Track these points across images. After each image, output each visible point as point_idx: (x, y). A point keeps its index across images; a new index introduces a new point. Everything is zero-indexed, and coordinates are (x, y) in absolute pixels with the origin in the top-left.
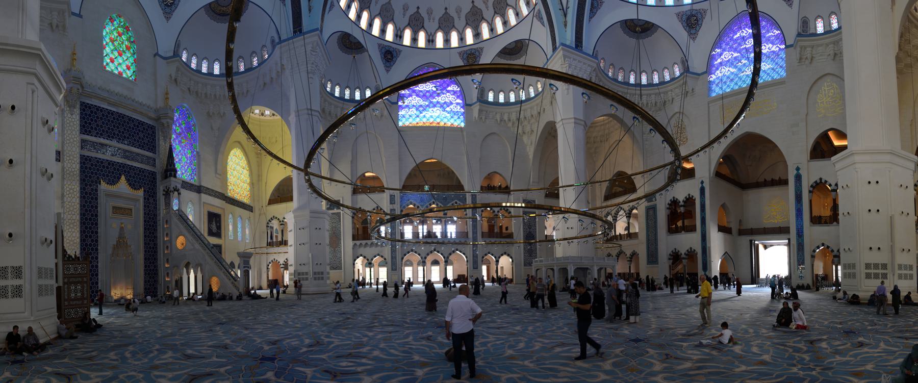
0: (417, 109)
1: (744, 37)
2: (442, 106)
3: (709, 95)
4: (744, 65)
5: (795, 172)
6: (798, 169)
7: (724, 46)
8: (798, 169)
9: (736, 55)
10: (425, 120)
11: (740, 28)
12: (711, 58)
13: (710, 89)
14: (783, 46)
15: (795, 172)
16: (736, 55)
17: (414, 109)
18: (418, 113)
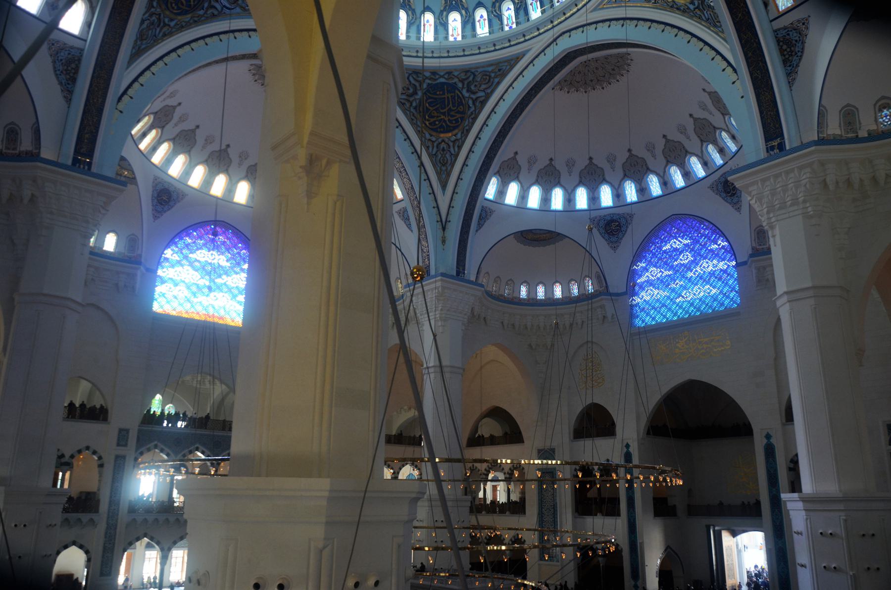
0: (188, 288)
1: (676, 250)
2: (230, 290)
3: (631, 324)
4: (681, 286)
5: (765, 441)
6: (768, 436)
7: (649, 256)
8: (768, 436)
9: (667, 273)
10: (199, 308)
11: (671, 237)
12: (632, 275)
13: (632, 316)
14: (734, 263)
15: (765, 441)
16: (667, 273)
17: (182, 287)
18: (189, 295)
